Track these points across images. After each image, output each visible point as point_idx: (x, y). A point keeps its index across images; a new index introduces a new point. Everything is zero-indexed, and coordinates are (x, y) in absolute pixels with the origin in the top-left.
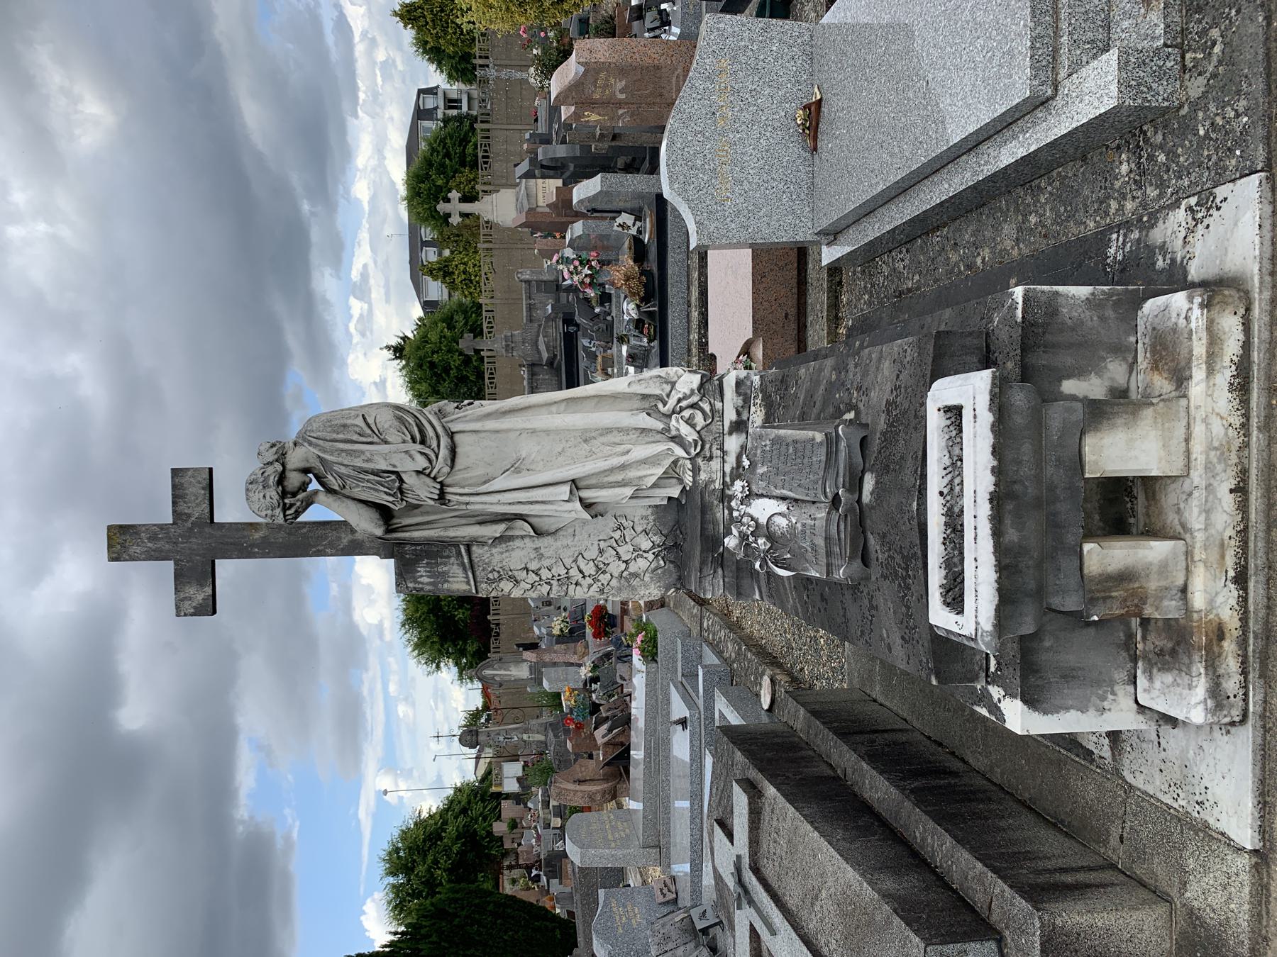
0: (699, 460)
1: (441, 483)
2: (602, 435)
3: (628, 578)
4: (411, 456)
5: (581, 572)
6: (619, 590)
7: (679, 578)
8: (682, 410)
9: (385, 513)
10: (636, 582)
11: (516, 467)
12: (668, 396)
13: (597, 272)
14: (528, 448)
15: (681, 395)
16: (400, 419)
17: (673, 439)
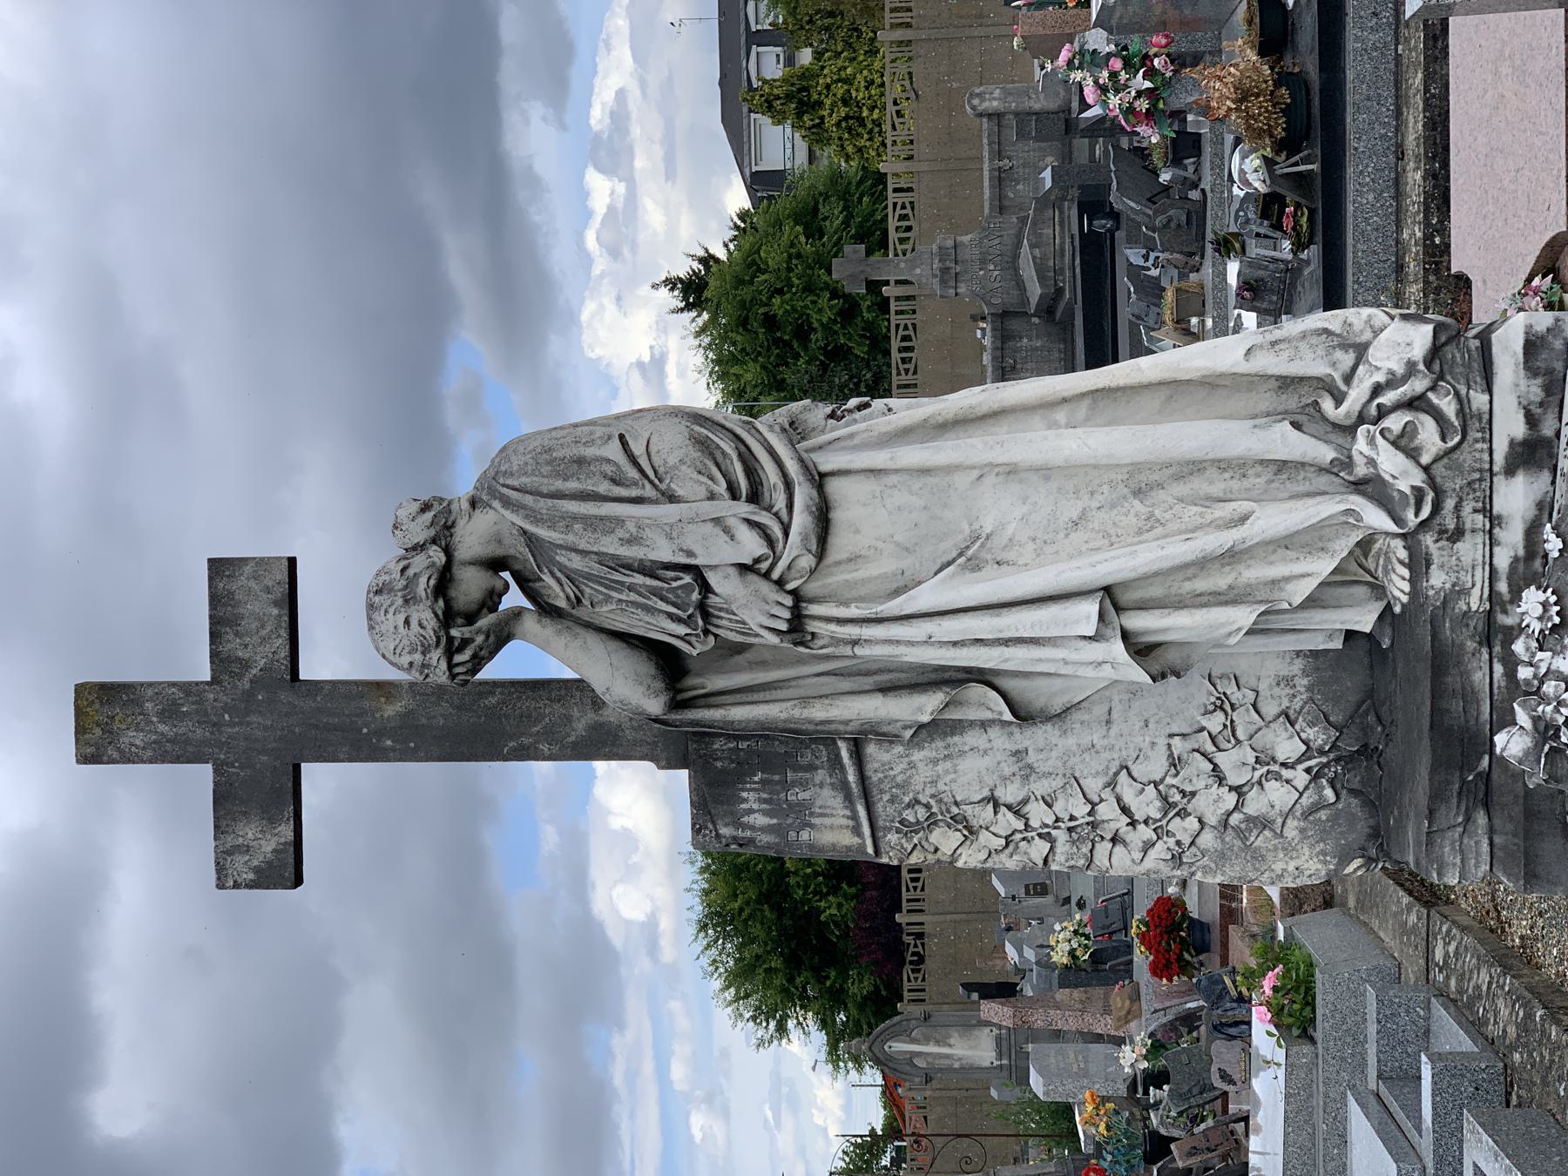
0: (1428, 540)
1: (794, 593)
2: (1179, 477)
3: (1243, 829)
4: (727, 531)
5: (1125, 810)
6: (1222, 857)
7: (1375, 834)
8: (1383, 412)
9: (668, 663)
10: (1262, 840)
11: (969, 556)
12: (1348, 378)
13: (1167, 83)
14: (998, 511)
15: (1380, 378)
16: (703, 445)
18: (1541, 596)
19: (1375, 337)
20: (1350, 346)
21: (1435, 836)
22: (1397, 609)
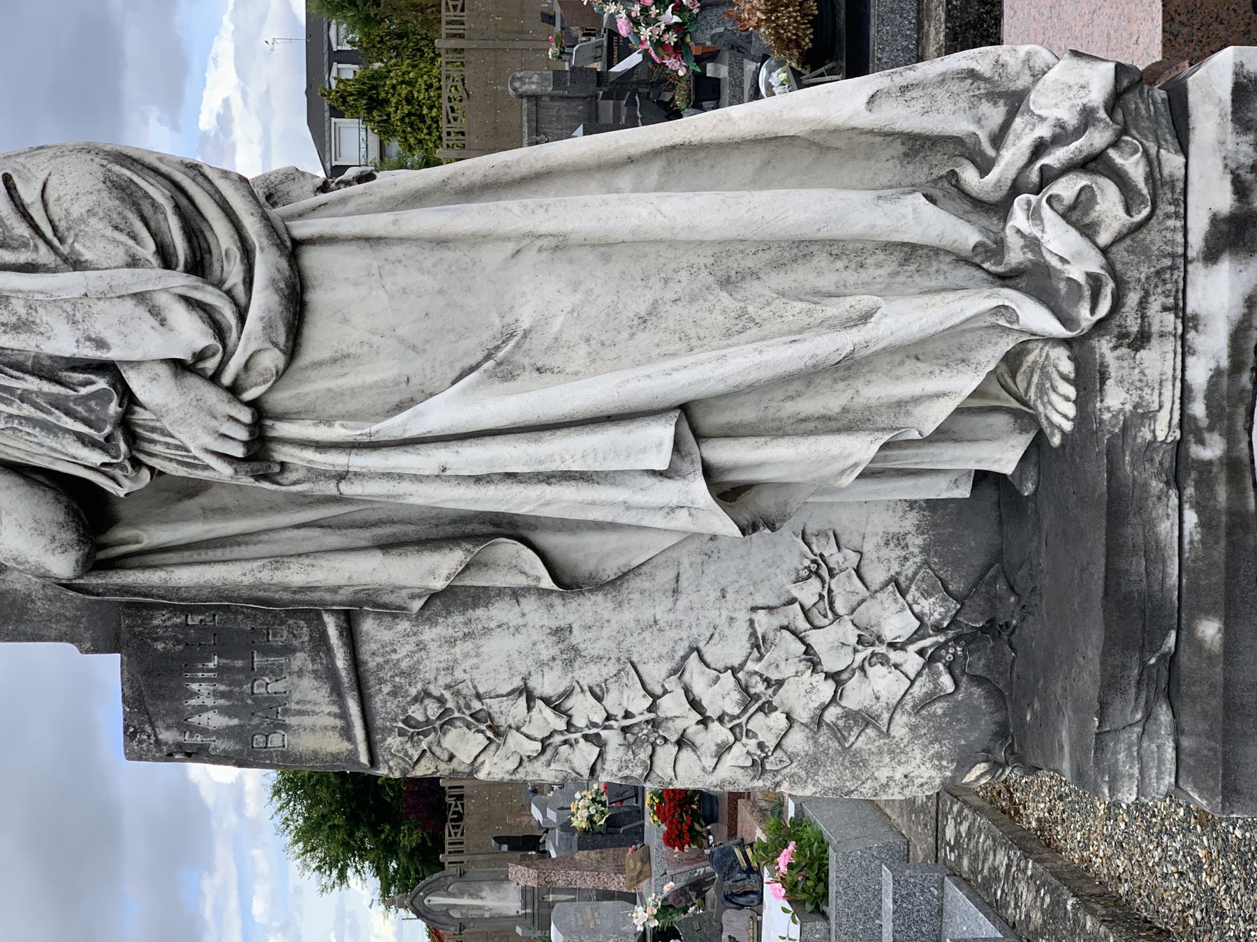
0: (1104, 346)
1: (254, 404)
2: (778, 265)
3: (841, 727)
4: (155, 312)
5: (695, 704)
6: (814, 762)
7: (1002, 732)
8: (1048, 177)
9: (87, 511)
10: (863, 741)
11: (500, 362)
12: (998, 139)
13: (694, 19)
14: (541, 300)
15: (1044, 131)
16: (126, 193)
17: (1006, 279)
19: (1035, 82)
20: (1001, 95)
22: (1056, 440)
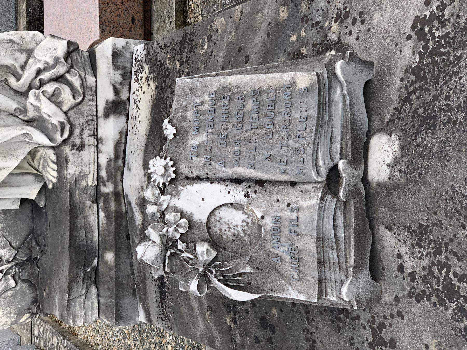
0: (67, 149)
7: (35, 301)
12: (23, 67)
15: (41, 65)
17: (29, 122)
18: (163, 162)
19: (37, 46)
20: (24, 50)
21: (72, 301)
22: (50, 186)
